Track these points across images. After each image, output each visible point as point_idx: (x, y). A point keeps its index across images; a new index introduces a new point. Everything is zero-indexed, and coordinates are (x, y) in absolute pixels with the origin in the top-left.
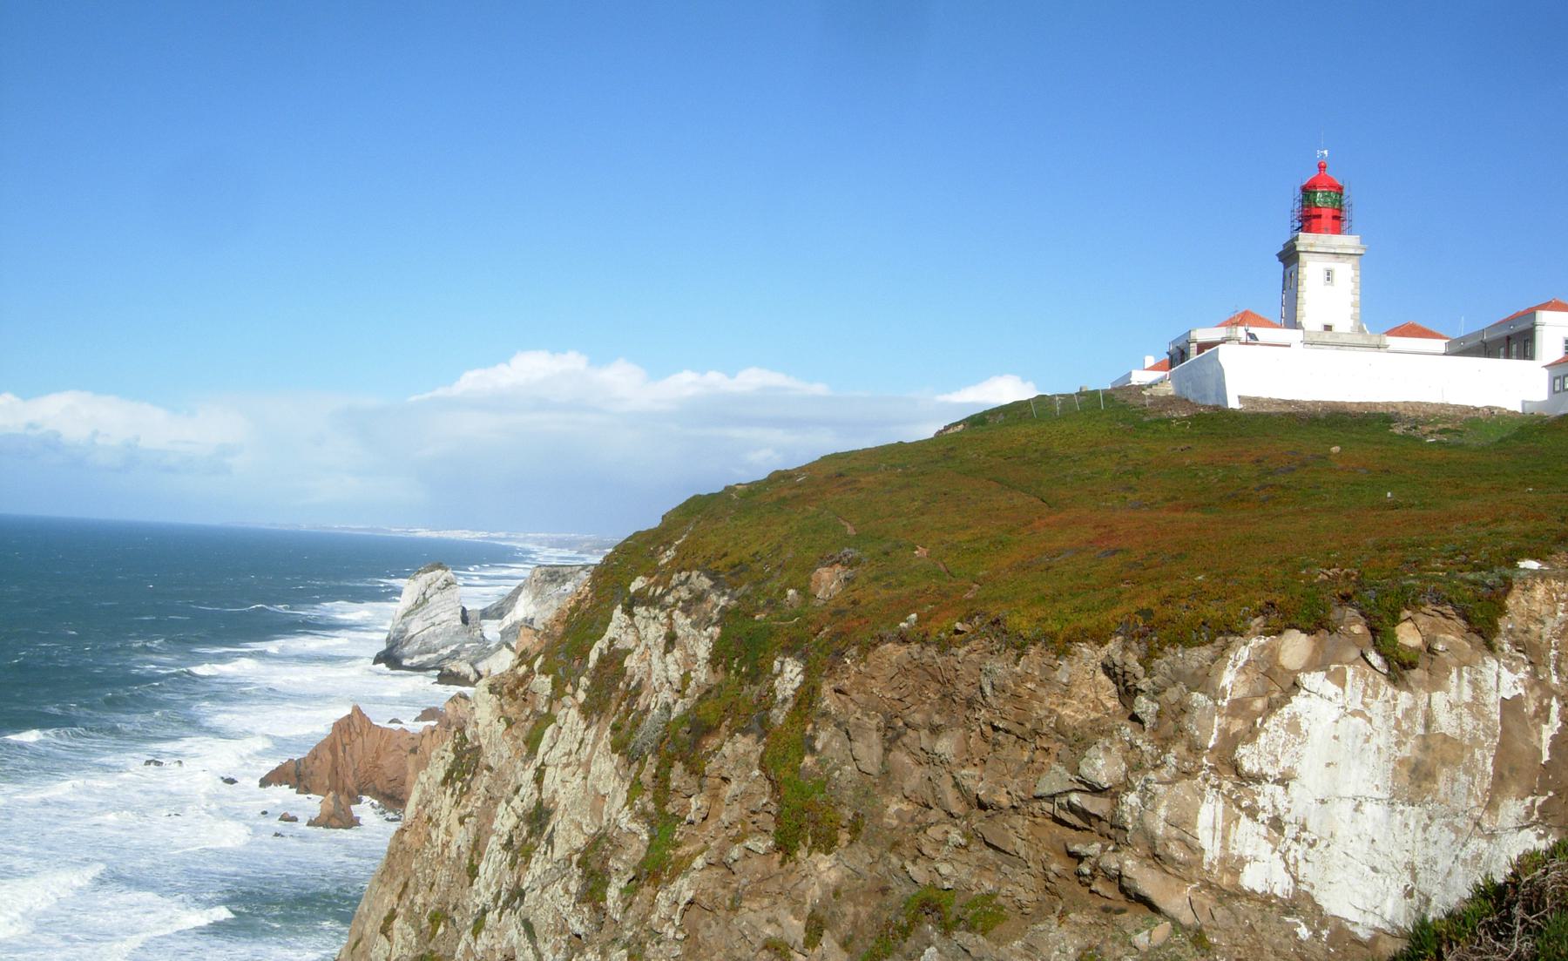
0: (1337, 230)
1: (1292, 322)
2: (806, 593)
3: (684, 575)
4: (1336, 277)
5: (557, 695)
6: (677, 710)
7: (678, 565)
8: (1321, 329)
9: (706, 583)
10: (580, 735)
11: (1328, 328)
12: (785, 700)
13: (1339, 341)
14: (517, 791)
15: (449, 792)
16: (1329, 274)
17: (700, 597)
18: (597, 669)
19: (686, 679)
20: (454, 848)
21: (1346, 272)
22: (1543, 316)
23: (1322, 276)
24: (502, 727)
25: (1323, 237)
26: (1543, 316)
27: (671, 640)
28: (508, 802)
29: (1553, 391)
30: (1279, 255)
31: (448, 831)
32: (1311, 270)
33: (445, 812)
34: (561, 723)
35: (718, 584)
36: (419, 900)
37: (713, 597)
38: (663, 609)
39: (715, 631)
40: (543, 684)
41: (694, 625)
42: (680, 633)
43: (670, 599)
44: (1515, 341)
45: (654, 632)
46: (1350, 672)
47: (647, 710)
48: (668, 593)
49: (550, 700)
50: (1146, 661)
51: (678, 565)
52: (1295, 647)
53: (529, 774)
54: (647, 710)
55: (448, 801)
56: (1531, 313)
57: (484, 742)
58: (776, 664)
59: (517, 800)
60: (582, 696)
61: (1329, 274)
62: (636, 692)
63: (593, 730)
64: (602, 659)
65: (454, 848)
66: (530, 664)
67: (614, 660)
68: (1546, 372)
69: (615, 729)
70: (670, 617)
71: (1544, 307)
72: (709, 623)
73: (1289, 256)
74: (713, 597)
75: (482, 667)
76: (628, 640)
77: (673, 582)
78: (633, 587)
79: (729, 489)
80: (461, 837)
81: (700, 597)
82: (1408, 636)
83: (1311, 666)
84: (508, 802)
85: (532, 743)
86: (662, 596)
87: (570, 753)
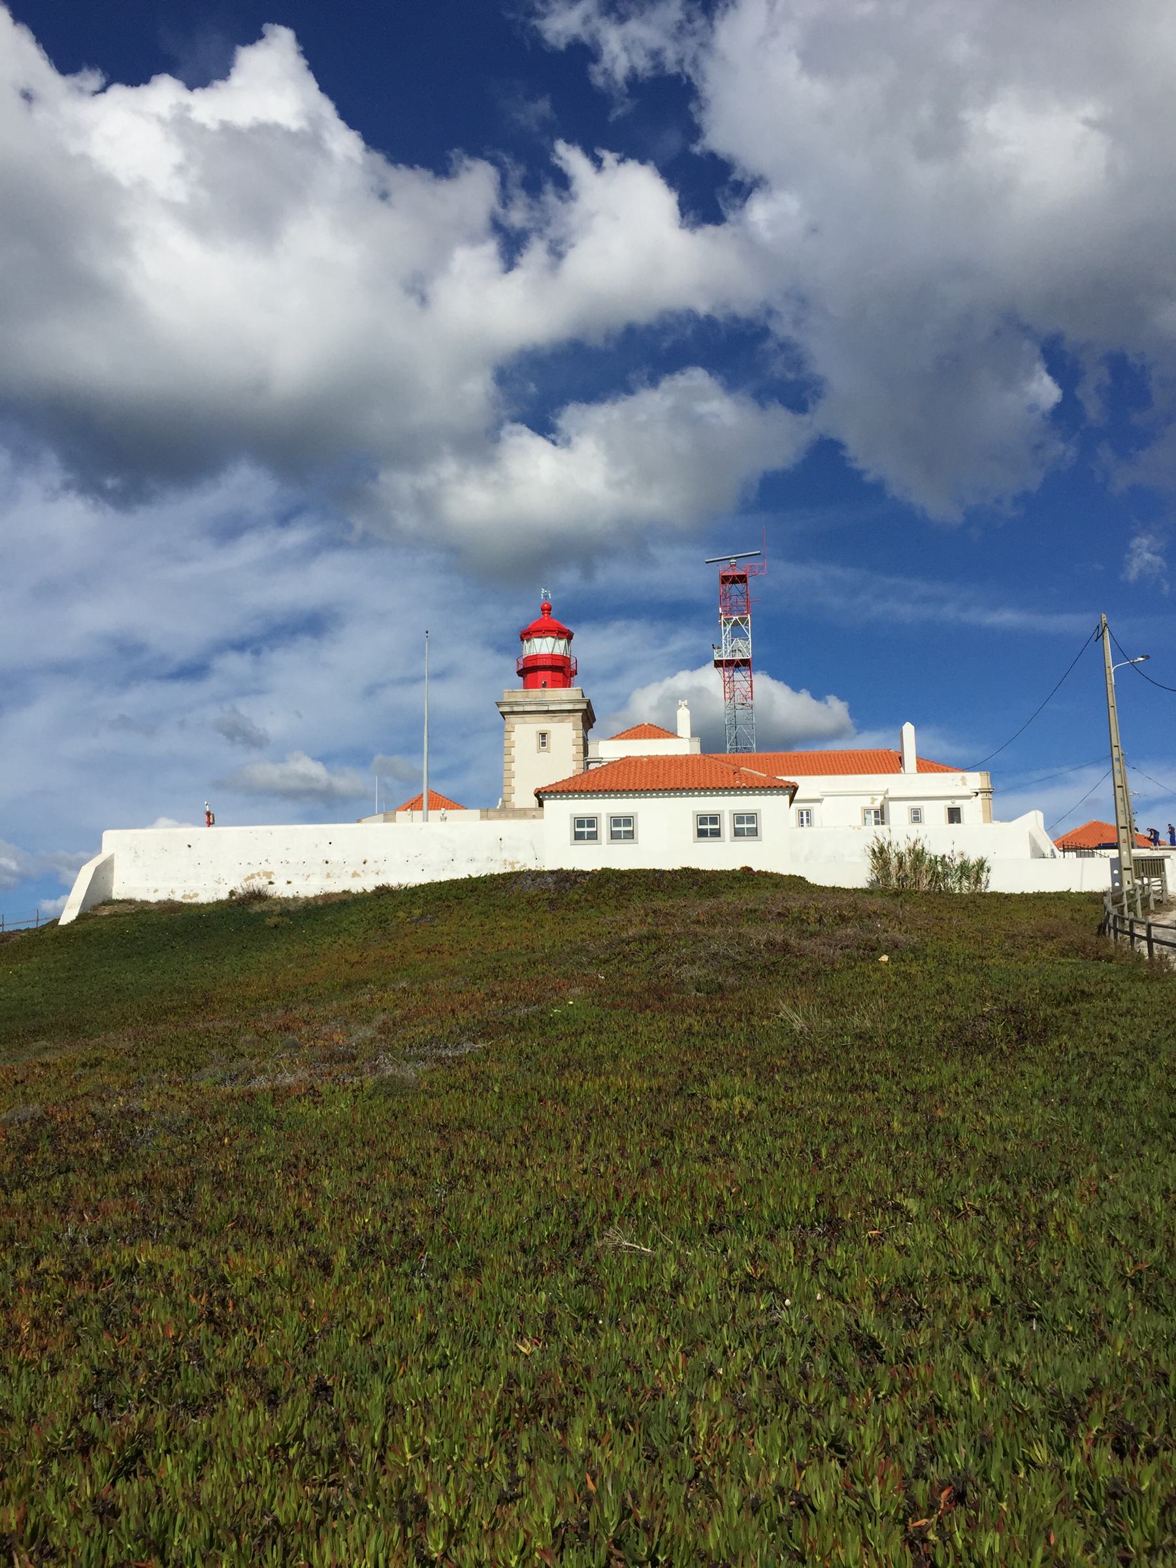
4: (552, 740)
21: (566, 732)
23: (535, 740)
25: (536, 693)
32: (523, 732)
61: (543, 735)
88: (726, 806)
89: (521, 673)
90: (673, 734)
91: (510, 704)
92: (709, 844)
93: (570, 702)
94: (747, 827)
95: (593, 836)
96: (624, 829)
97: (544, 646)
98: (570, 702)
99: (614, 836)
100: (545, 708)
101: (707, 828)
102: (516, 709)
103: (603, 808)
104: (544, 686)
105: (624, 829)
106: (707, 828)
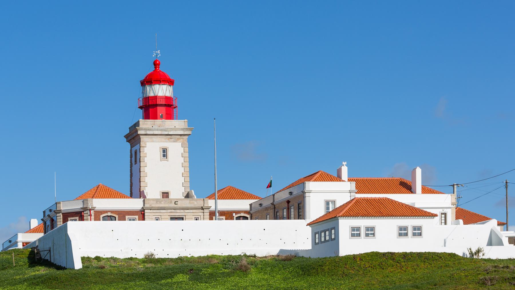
0: (169, 116)
1: (135, 190)
4: (169, 153)
8: (159, 196)
11: (165, 195)
13: (173, 205)
16: (165, 152)
21: (177, 150)
22: (311, 186)
23: (159, 154)
25: (158, 122)
26: (311, 186)
29: (314, 243)
30: (126, 137)
32: (150, 149)
44: (292, 207)
56: (301, 182)
61: (165, 152)
68: (309, 229)
71: (310, 178)
73: (133, 138)
88: (410, 222)
89: (141, 108)
90: (339, 178)
91: (146, 129)
92: (403, 239)
93: (183, 129)
94: (418, 232)
95: (359, 235)
96: (371, 232)
97: (161, 90)
98: (183, 129)
99: (367, 235)
100: (166, 133)
101: (403, 232)
102: (148, 132)
103: (363, 223)
104: (162, 118)
105: (371, 232)
106: (403, 232)
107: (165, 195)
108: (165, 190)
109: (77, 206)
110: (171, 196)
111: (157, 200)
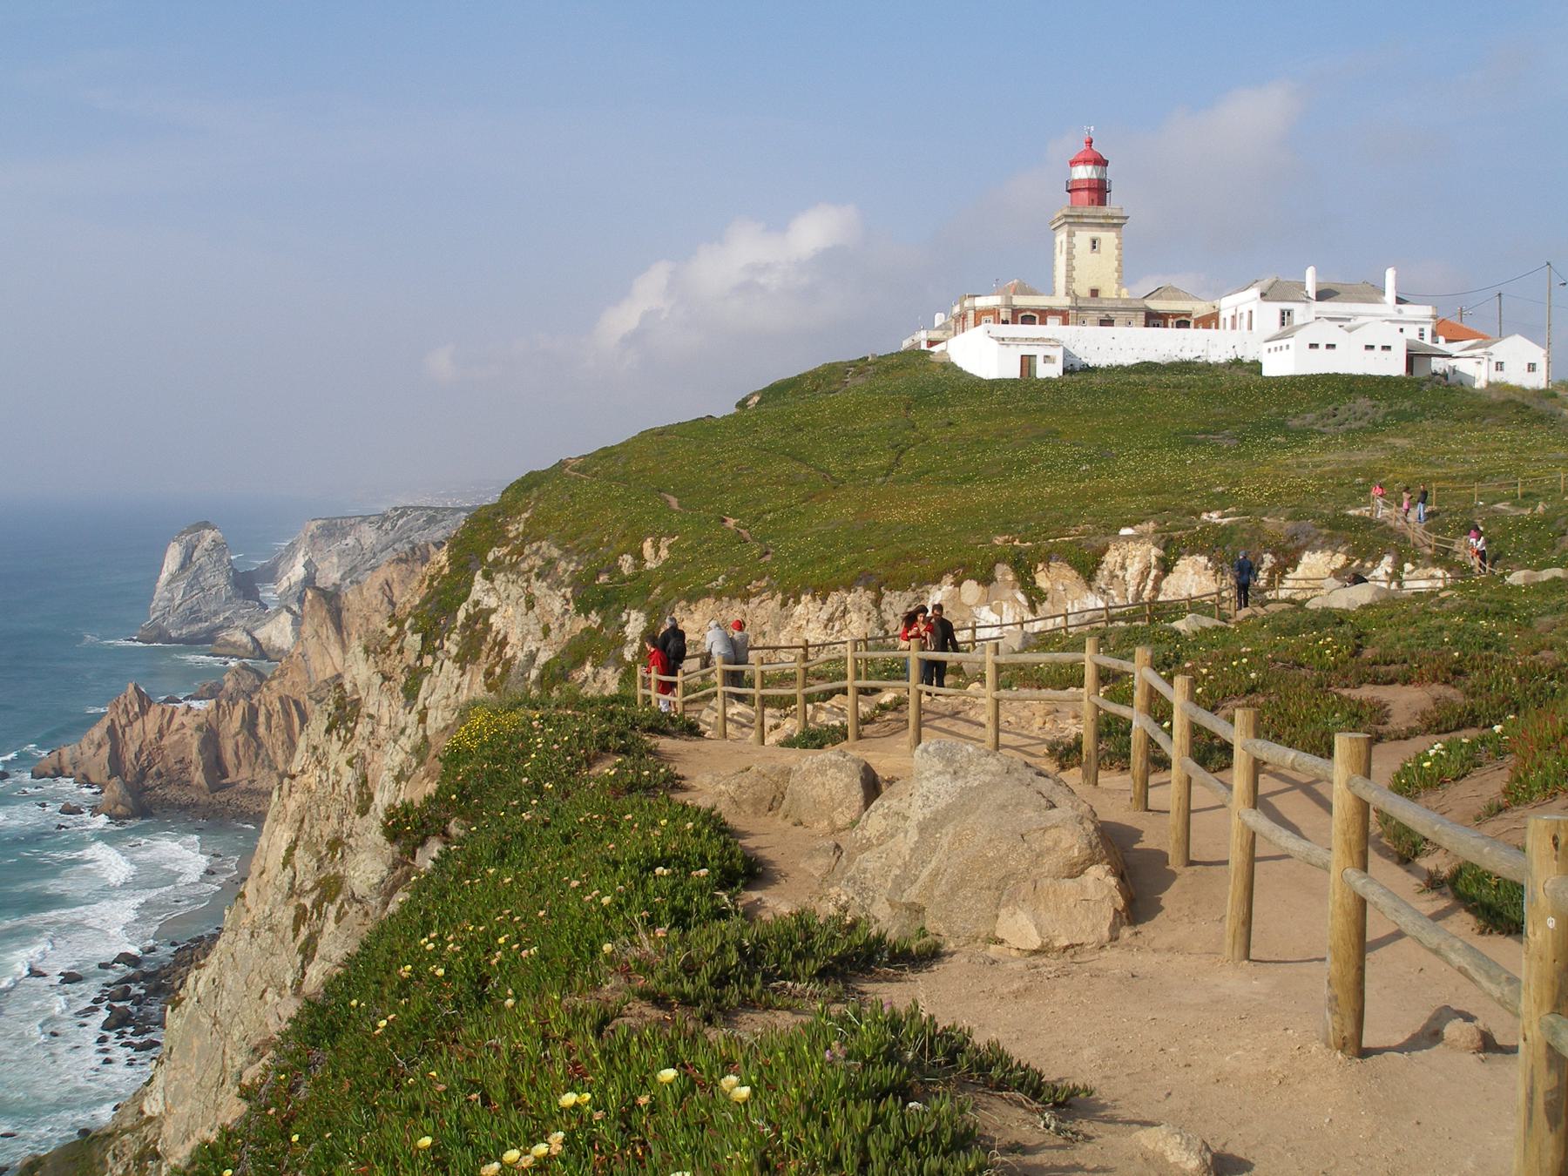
2: (639, 556)
3: (535, 546)
5: (428, 648)
6: (543, 658)
7: (528, 537)
9: (556, 553)
10: (456, 682)
11: (1095, 293)
12: (633, 641)
14: (403, 731)
15: (335, 737)
17: (551, 562)
18: (464, 626)
19: (546, 631)
20: (344, 786)
24: (377, 680)
27: (530, 604)
28: (395, 742)
31: (336, 771)
33: (332, 756)
34: (436, 672)
35: (567, 553)
36: (317, 833)
37: (563, 564)
38: (520, 574)
39: (568, 592)
40: (414, 641)
41: (550, 587)
42: (537, 593)
43: (524, 566)
45: (515, 591)
46: (1005, 606)
47: (514, 657)
48: (523, 560)
49: (420, 657)
50: (877, 603)
51: (528, 537)
52: (971, 589)
53: (414, 717)
54: (514, 657)
55: (336, 745)
57: (363, 694)
58: (624, 617)
59: (403, 740)
60: (454, 650)
62: (503, 643)
63: (467, 678)
64: (468, 617)
65: (344, 786)
66: (401, 624)
67: (481, 616)
69: (489, 673)
70: (528, 580)
72: (560, 584)
74: (563, 564)
75: (260, 634)
76: (490, 601)
77: (526, 552)
78: (490, 557)
79: (562, 464)
80: (348, 775)
81: (551, 562)
82: (1042, 581)
83: (980, 603)
84: (395, 742)
85: (411, 693)
86: (517, 563)
87: (448, 697)
107: (1095, 293)
108: (1094, 285)
109: (993, 301)
110: (1101, 295)
111: (1085, 299)
